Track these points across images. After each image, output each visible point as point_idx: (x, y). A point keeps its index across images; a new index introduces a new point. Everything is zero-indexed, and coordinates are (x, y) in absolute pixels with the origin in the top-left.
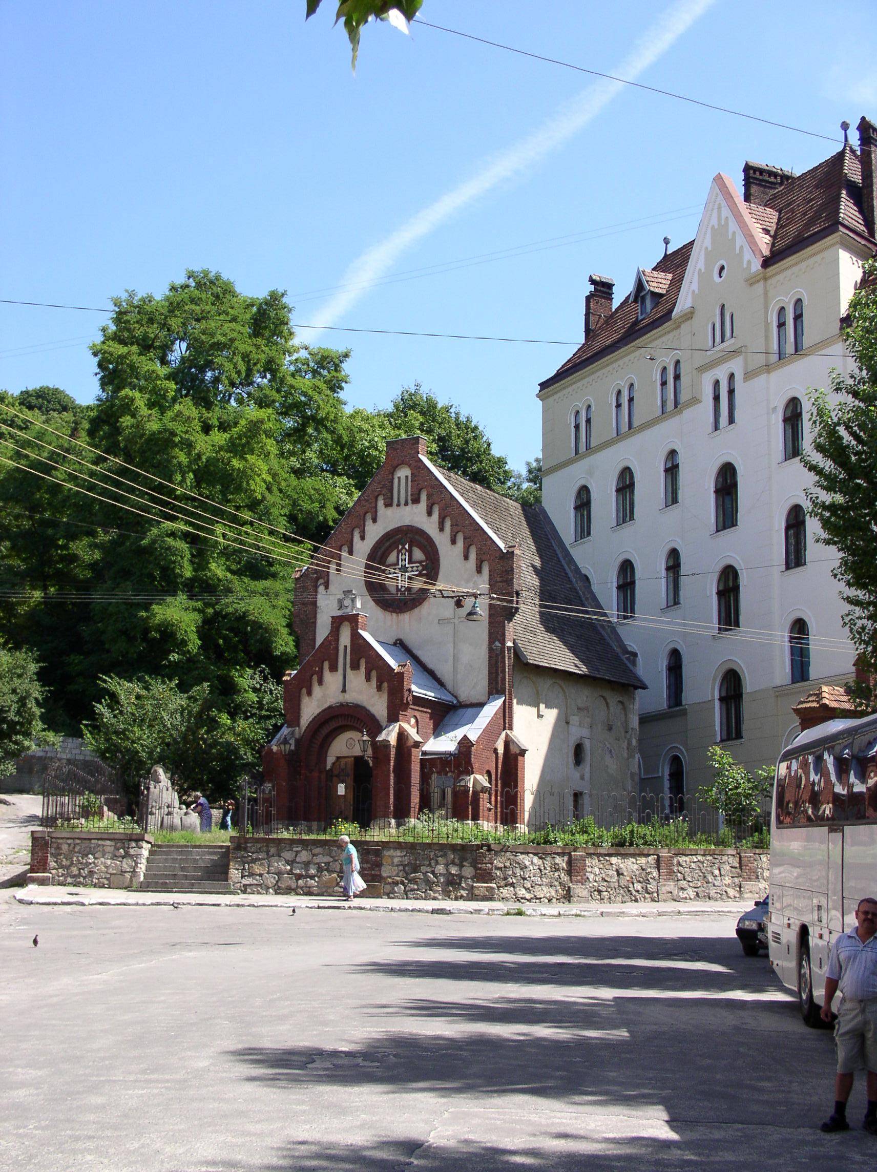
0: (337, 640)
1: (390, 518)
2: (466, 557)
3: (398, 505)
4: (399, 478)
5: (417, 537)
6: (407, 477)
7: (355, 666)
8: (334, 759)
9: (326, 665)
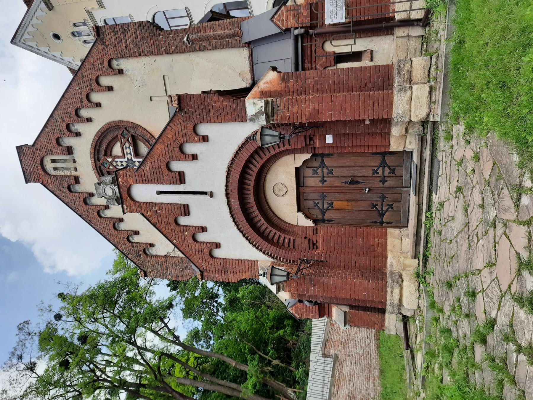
0: (150, 205)
1: (89, 180)
2: (110, 89)
3: (76, 170)
4: (55, 169)
5: (103, 149)
6: (53, 161)
7: (181, 178)
8: (300, 214)
9: (183, 221)
